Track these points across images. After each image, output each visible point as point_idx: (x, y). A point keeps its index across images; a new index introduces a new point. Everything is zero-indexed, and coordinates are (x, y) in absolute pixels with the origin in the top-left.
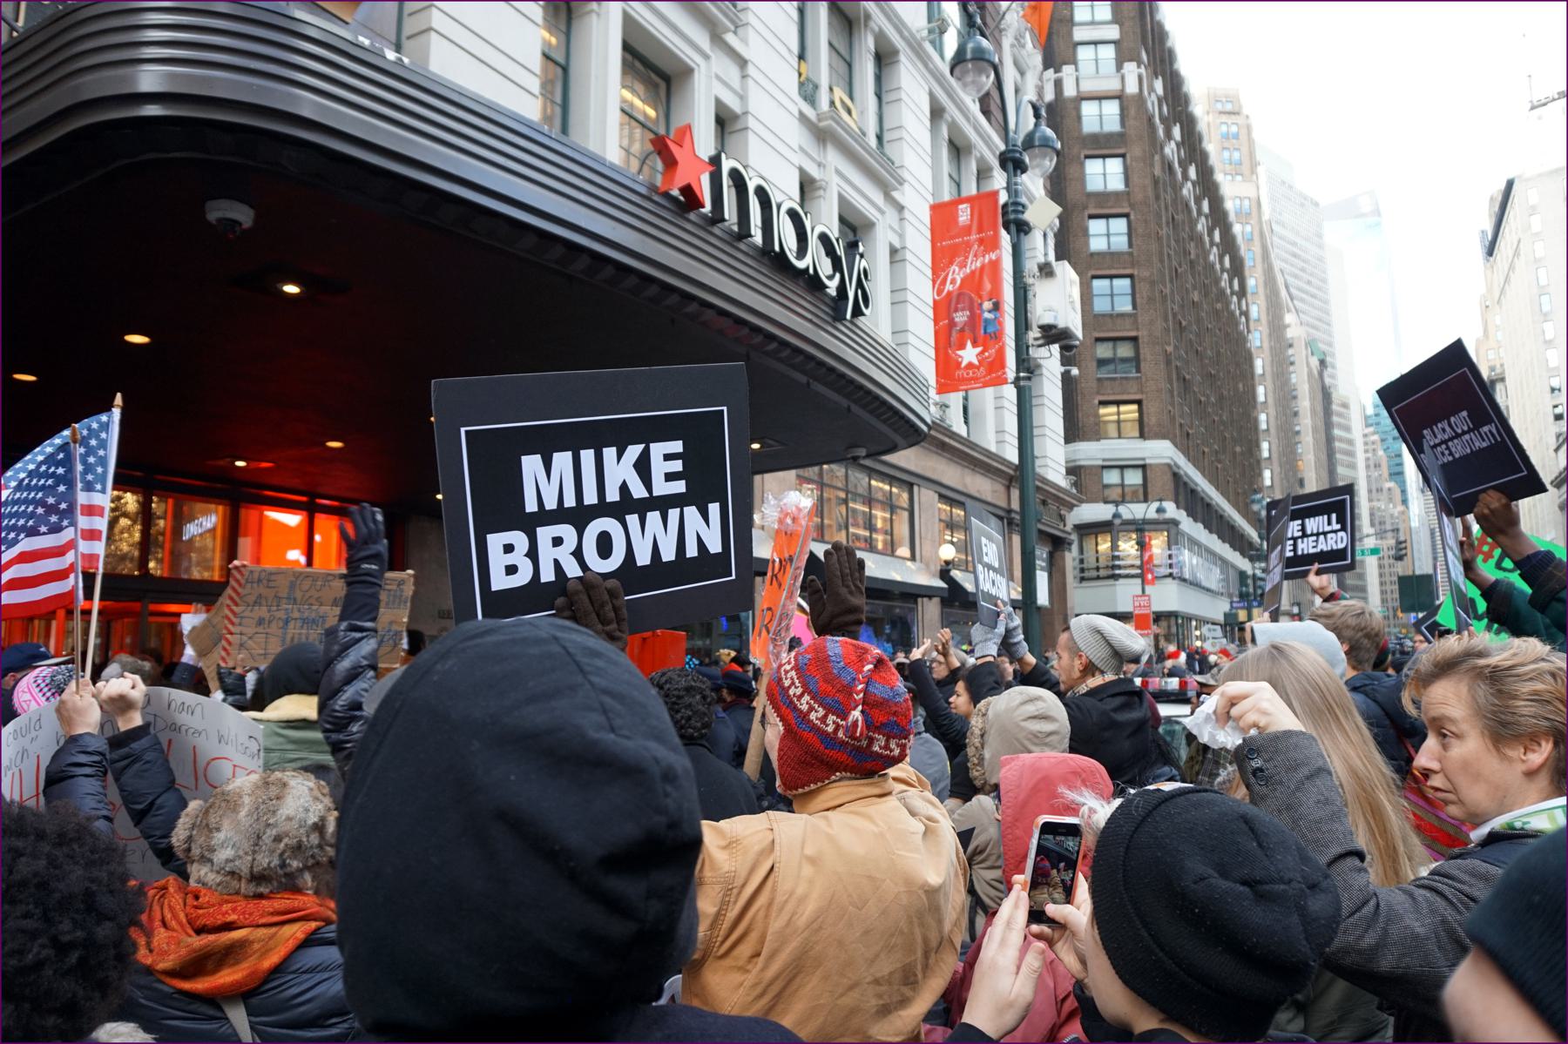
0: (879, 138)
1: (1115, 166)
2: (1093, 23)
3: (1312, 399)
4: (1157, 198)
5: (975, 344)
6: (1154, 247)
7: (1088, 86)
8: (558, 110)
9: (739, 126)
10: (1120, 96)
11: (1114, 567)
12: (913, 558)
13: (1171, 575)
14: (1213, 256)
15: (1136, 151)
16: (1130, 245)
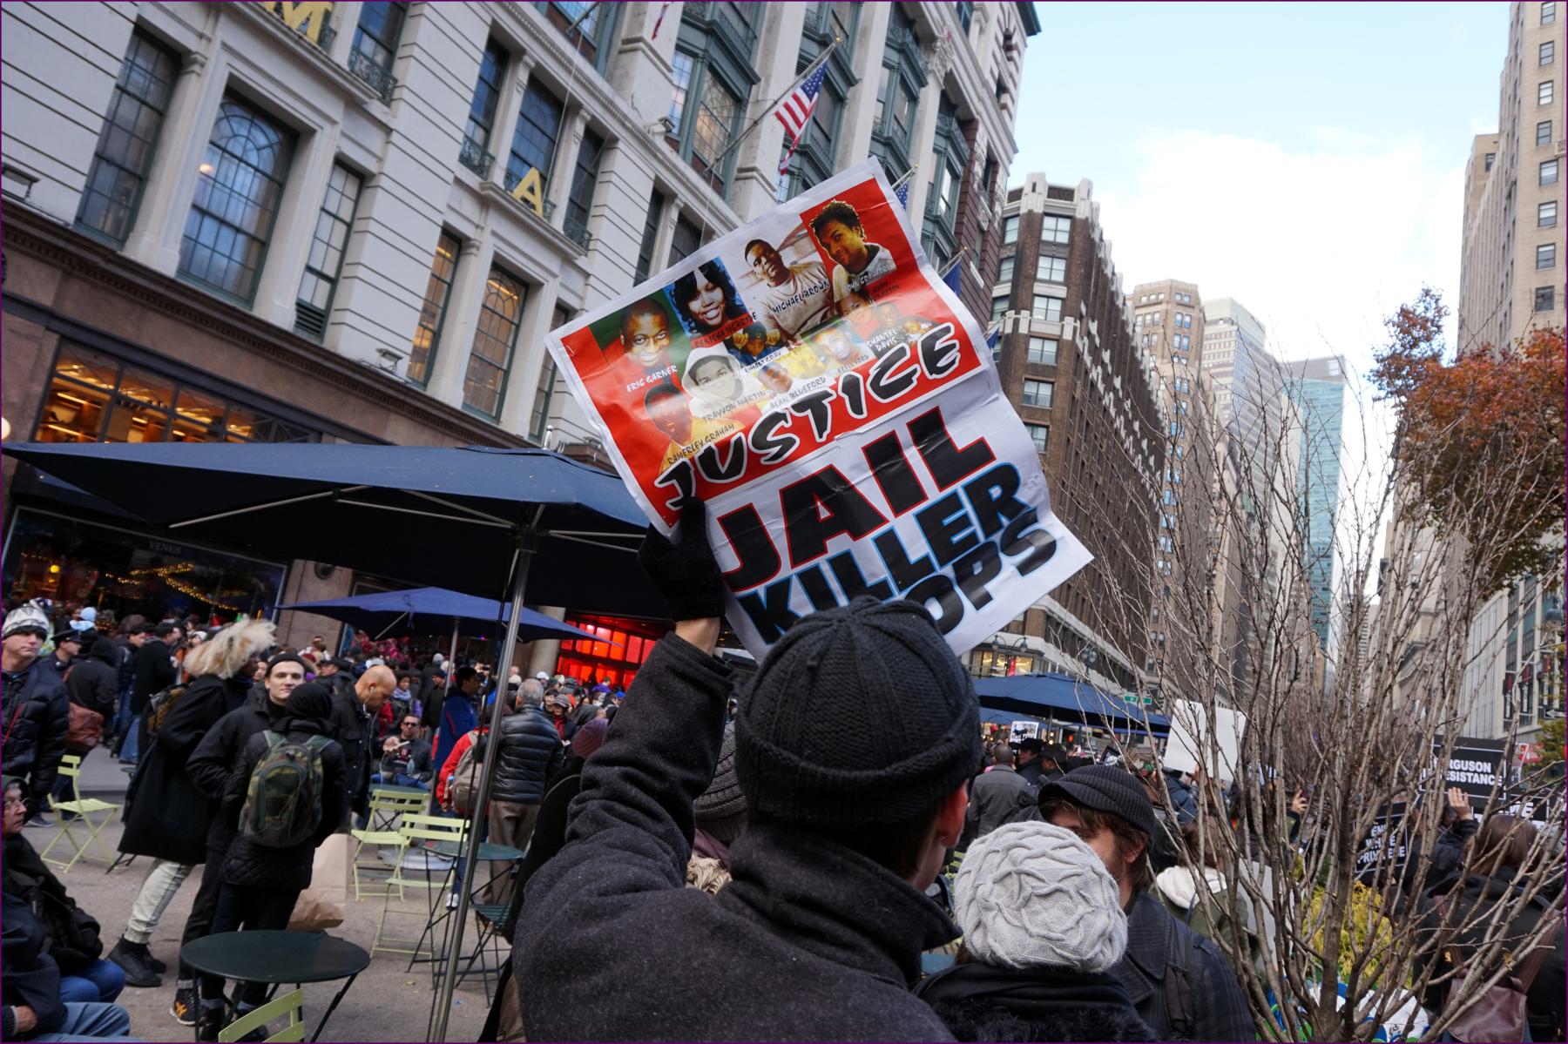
1: (1045, 390)
2: (1050, 282)
4: (1072, 414)
6: (1062, 453)
7: (1036, 328)
10: (1058, 340)
15: (1062, 382)
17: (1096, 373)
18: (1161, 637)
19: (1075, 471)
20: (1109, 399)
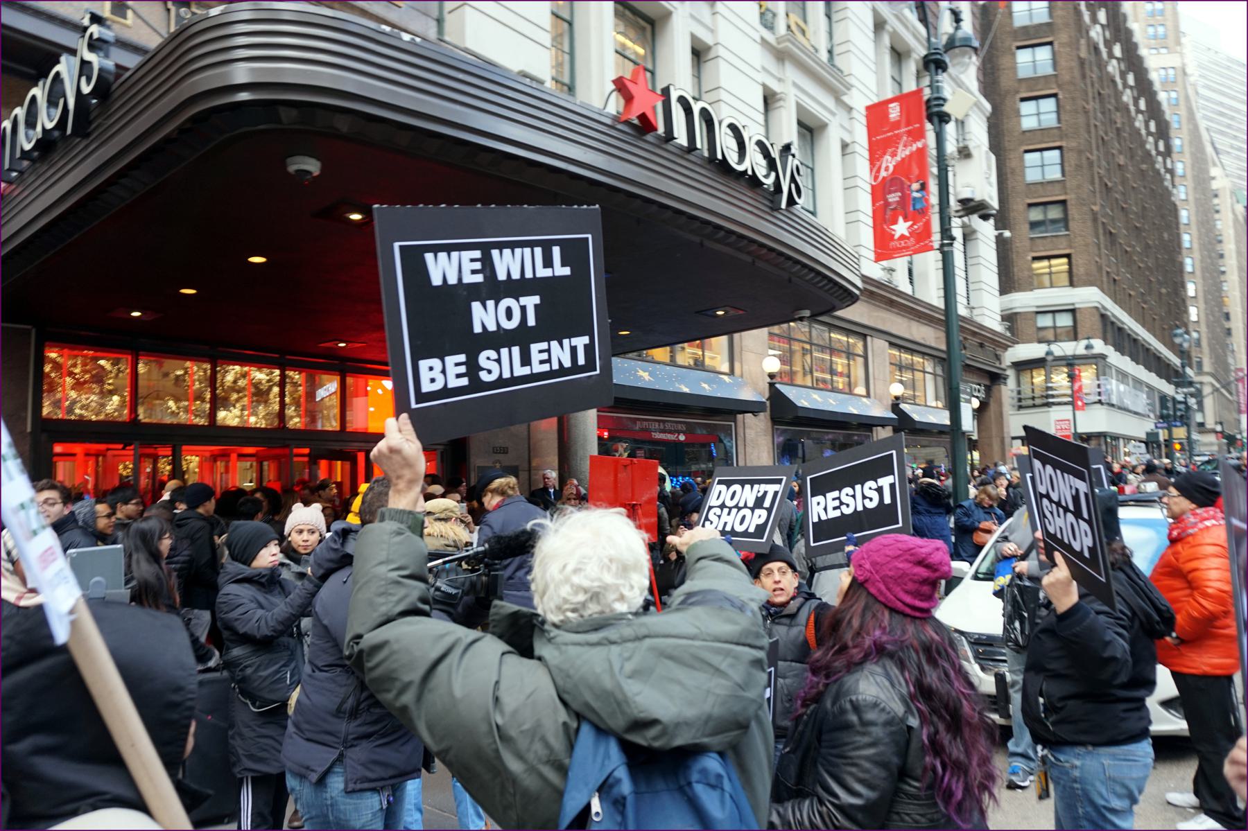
0: (830, 52)
1: (1044, 54)
3: (1237, 242)
4: (1084, 76)
5: (906, 220)
6: (1081, 120)
8: (567, 57)
9: (712, 55)
11: (1047, 397)
12: (868, 395)
13: (1100, 402)
14: (1139, 122)
16: (1059, 120)
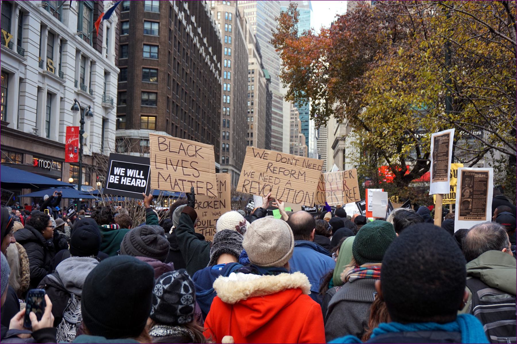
0: (60, 65)
1: (155, 27)
3: (260, 98)
6: (166, 60)
15: (164, 22)
17: (181, 16)
18: (227, 146)
19: (174, 68)
20: (189, 29)
